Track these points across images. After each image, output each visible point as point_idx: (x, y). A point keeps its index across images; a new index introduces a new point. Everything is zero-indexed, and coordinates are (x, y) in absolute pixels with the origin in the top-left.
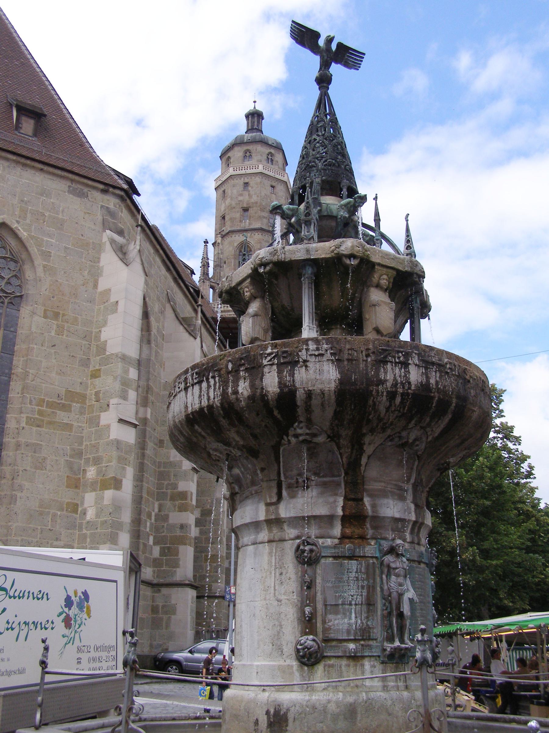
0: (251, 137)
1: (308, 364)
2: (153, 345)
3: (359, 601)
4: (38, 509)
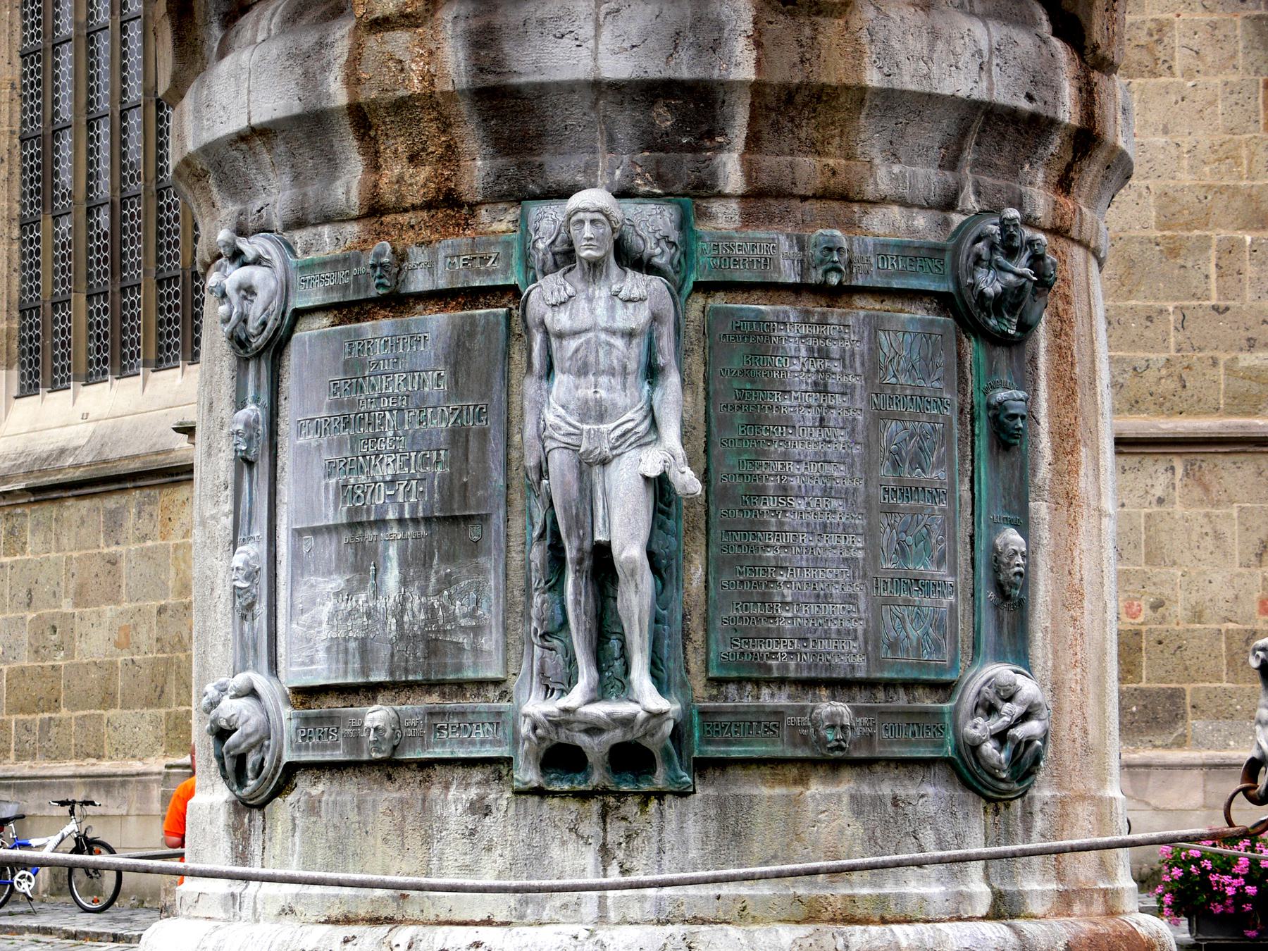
3: (414, 508)
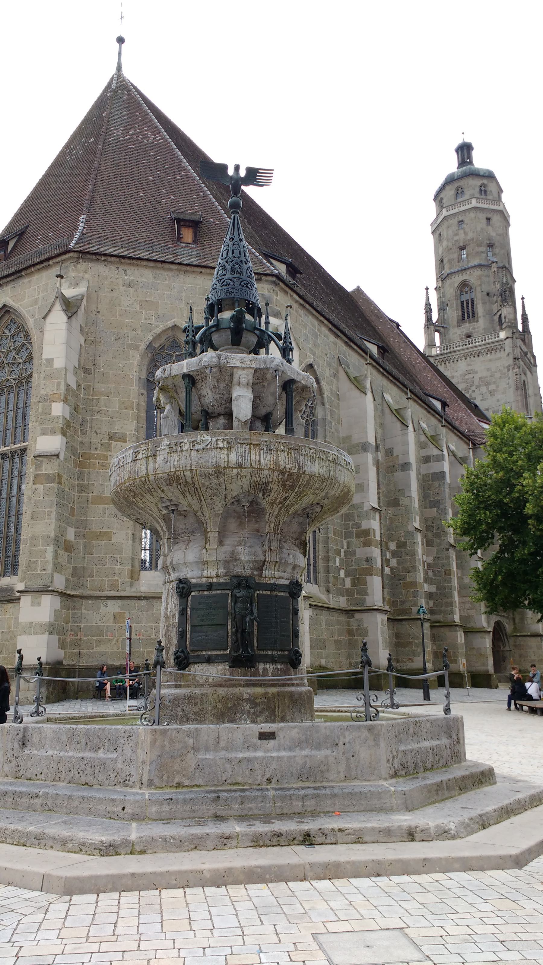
0: (461, 172)
2: (327, 405)
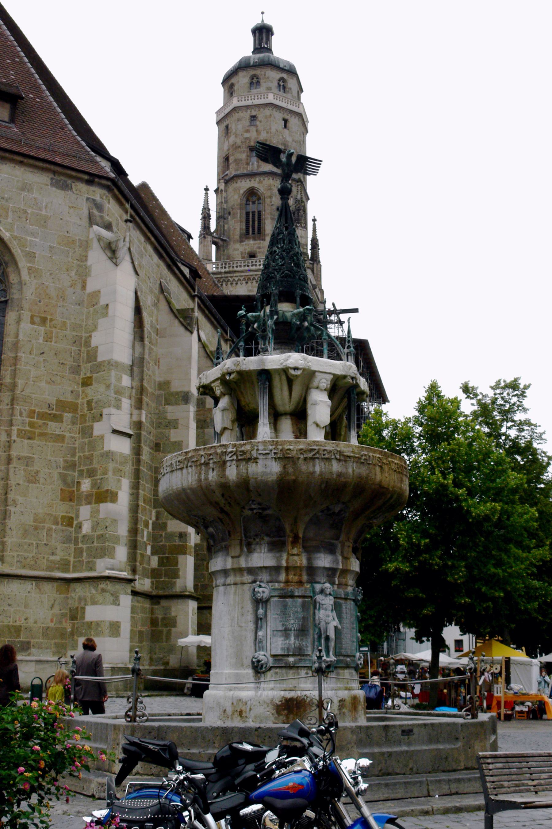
1: (258, 461)
2: (146, 342)
4: (33, 524)
